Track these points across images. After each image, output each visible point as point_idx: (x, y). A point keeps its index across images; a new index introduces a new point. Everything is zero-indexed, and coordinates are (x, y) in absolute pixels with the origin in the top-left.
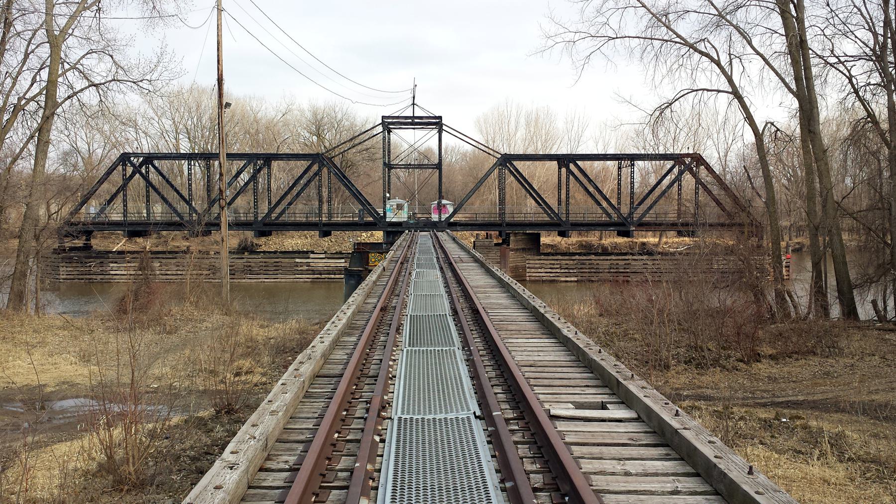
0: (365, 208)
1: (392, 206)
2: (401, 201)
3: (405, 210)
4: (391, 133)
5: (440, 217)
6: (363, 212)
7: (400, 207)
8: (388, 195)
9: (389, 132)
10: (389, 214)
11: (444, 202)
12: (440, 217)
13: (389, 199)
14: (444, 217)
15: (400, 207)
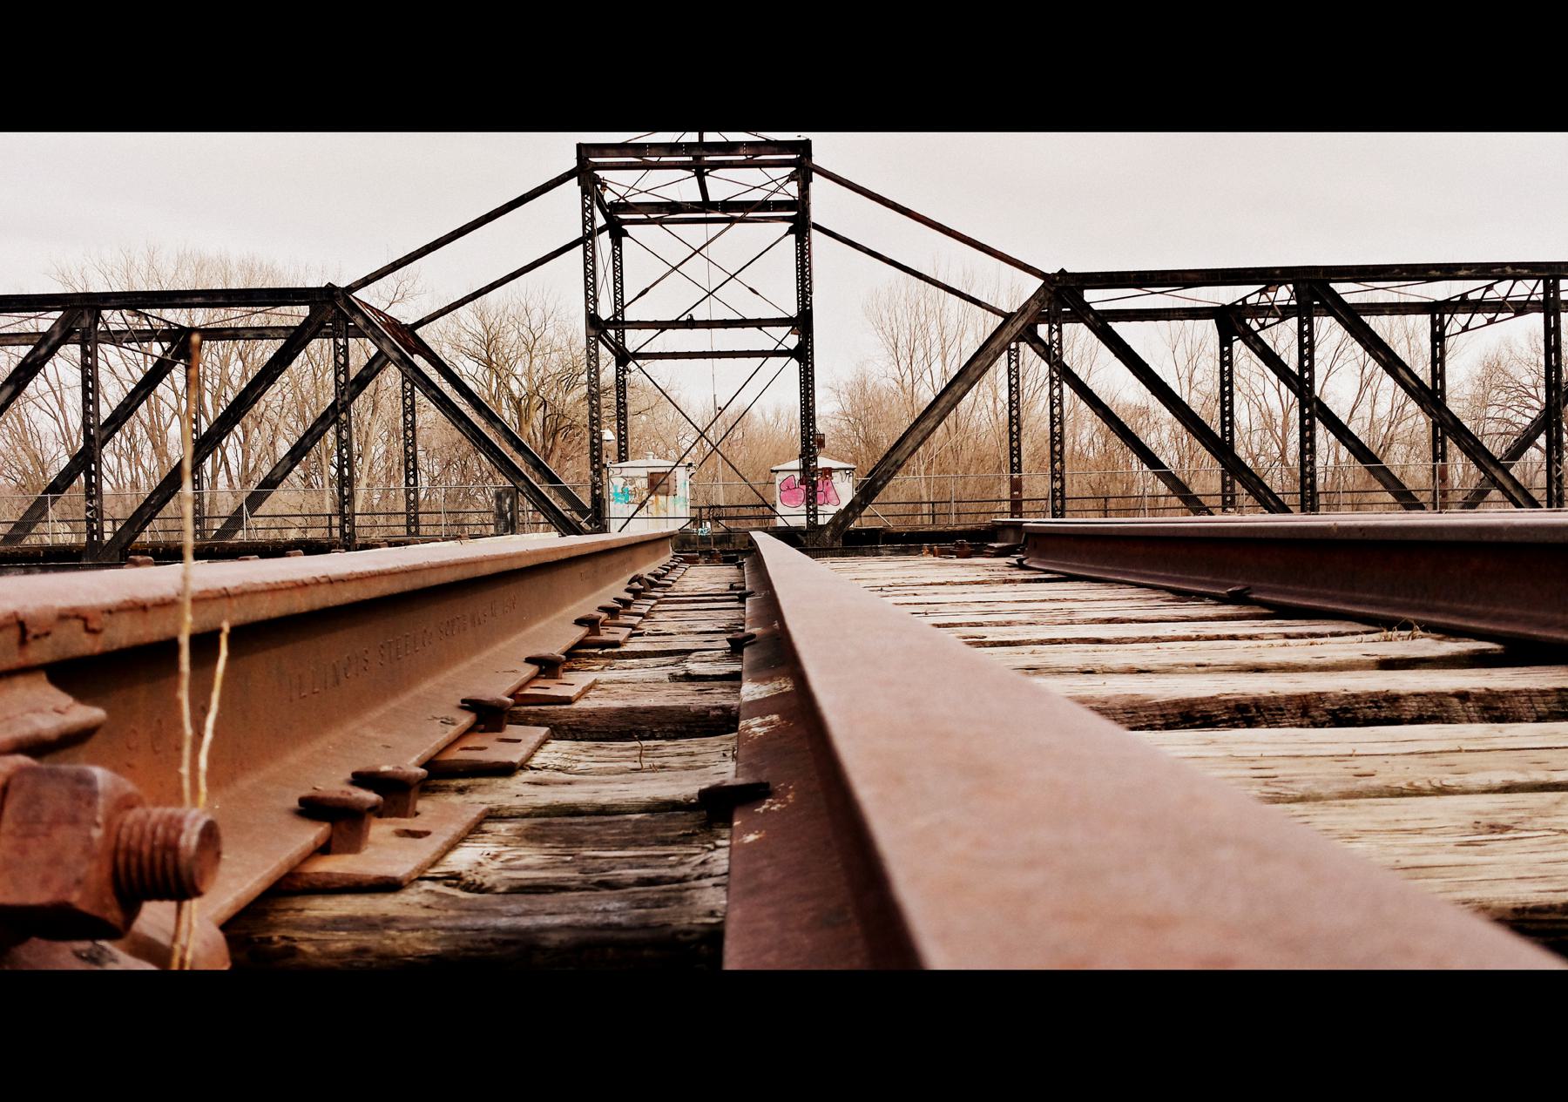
0: (521, 484)
1: (633, 480)
2: (661, 464)
3: (680, 493)
4: (624, 239)
5: (812, 513)
6: (514, 499)
7: (658, 483)
8: (609, 435)
9: (618, 235)
10: (617, 509)
11: (823, 462)
12: (812, 513)
13: (622, 456)
14: (827, 513)
15: (658, 483)
